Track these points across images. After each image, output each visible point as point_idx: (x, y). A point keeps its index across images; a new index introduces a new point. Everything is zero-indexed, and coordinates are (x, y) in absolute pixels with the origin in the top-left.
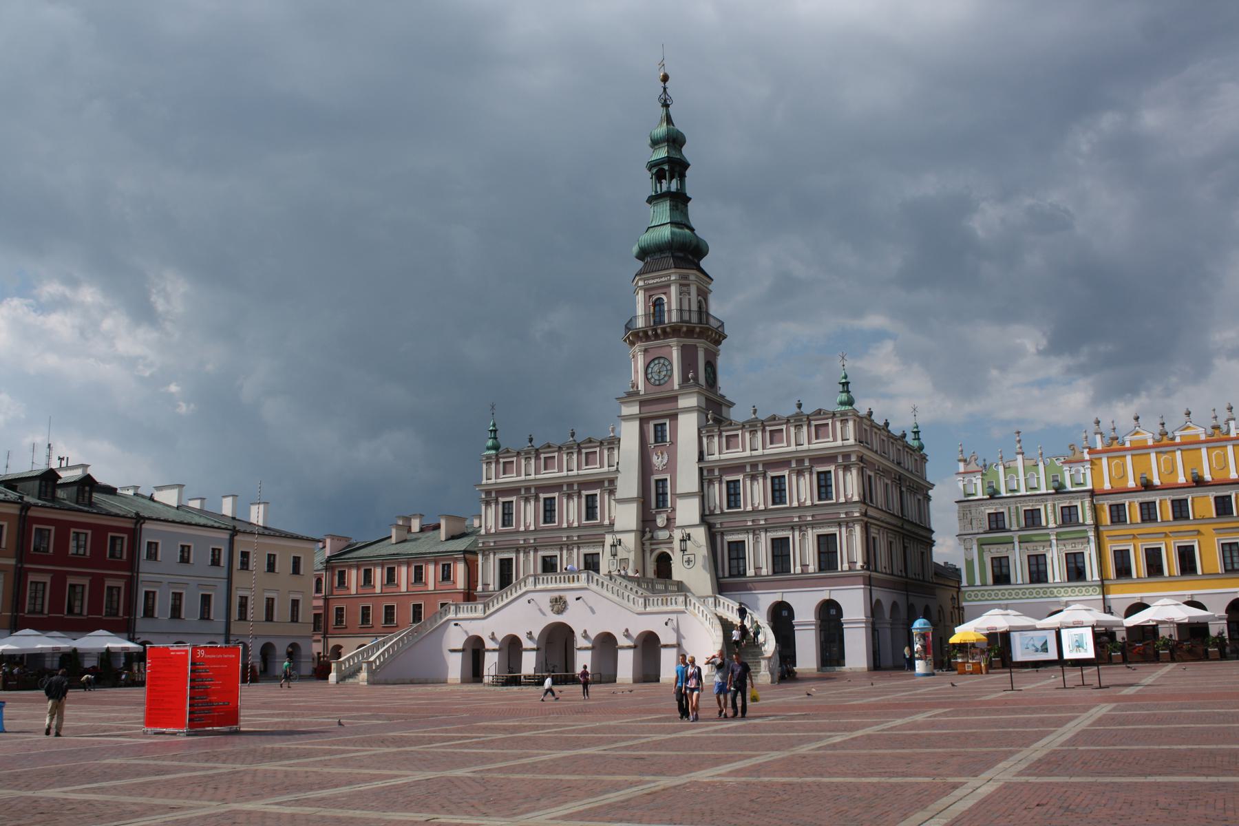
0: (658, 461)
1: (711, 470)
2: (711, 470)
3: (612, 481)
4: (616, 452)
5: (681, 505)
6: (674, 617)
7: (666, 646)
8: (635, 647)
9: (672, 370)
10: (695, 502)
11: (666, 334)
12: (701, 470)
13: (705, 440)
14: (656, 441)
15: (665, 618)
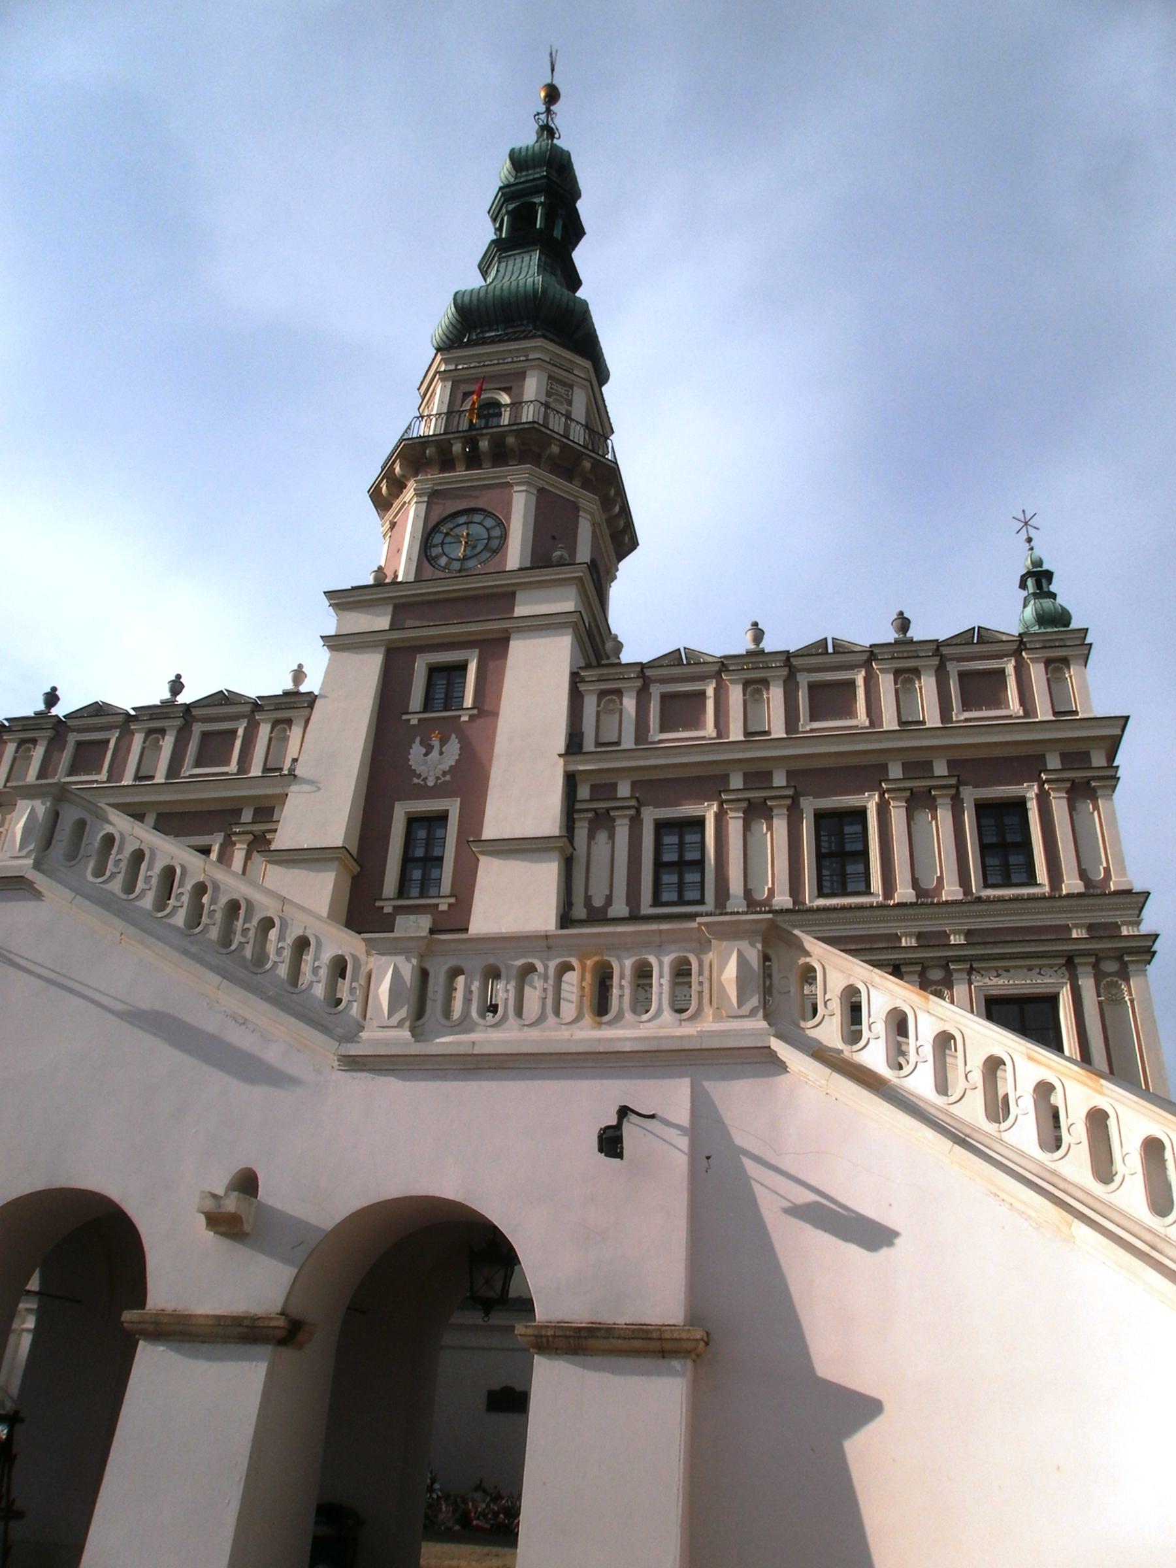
0: (431, 762)
1: (604, 789)
2: (604, 789)
3: (267, 811)
4: (295, 733)
5: (492, 875)
6: (672, 1098)
7: (581, 1342)
8: (281, 1334)
9: (504, 537)
10: (548, 872)
11: (501, 455)
12: (571, 780)
13: (590, 705)
14: (427, 707)
15: (593, 1101)
